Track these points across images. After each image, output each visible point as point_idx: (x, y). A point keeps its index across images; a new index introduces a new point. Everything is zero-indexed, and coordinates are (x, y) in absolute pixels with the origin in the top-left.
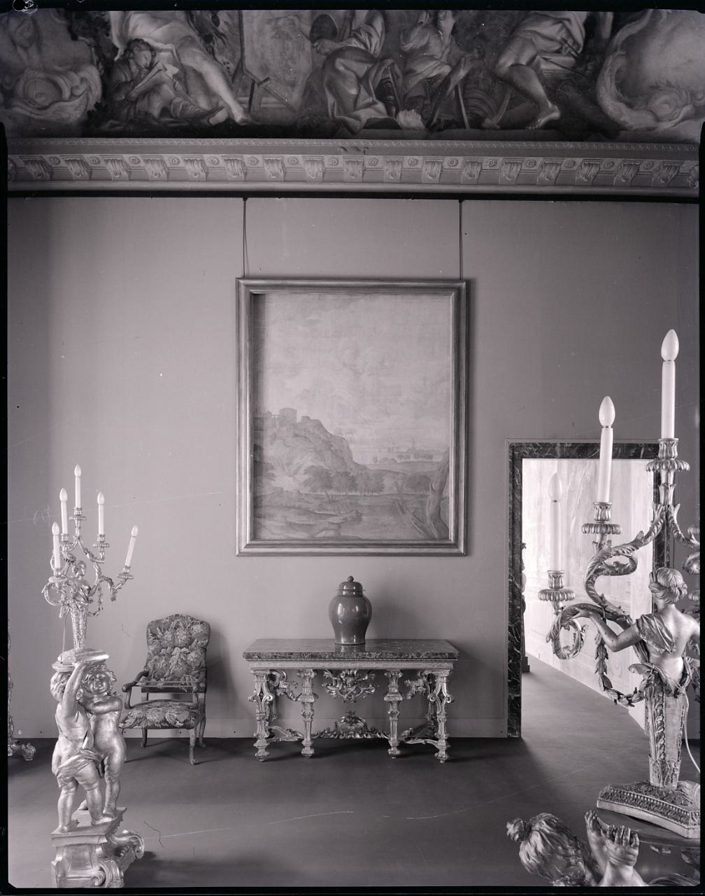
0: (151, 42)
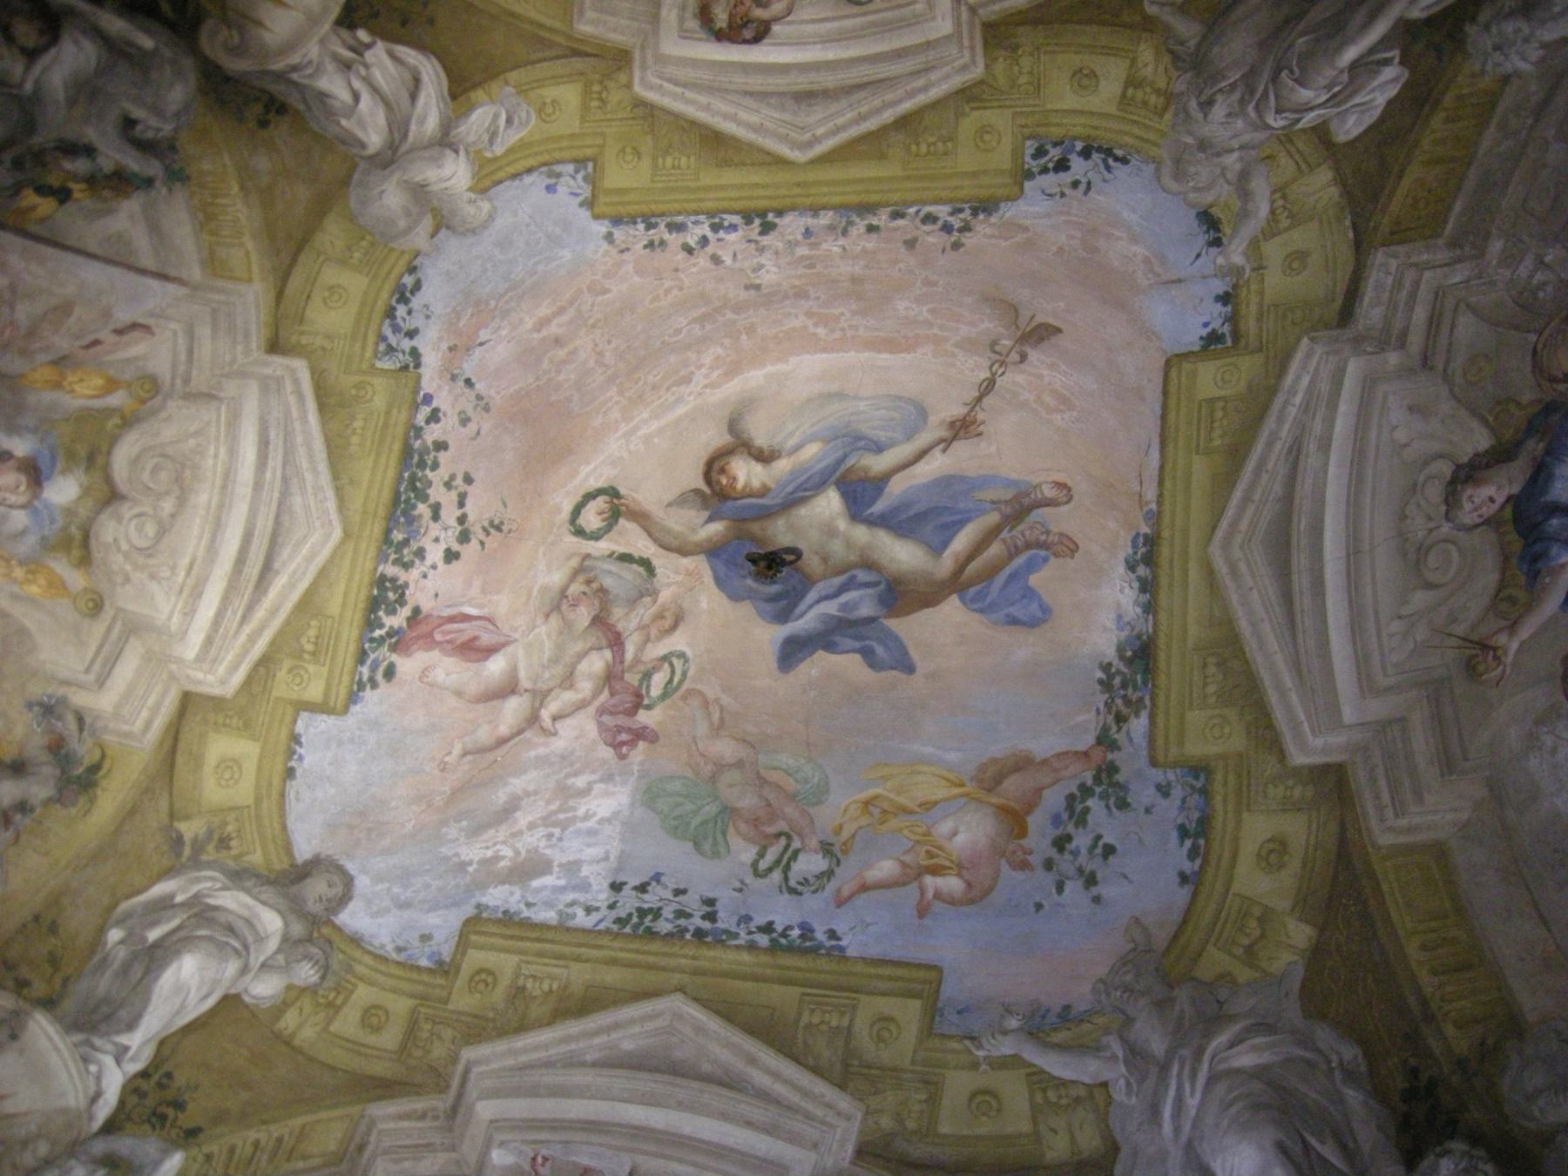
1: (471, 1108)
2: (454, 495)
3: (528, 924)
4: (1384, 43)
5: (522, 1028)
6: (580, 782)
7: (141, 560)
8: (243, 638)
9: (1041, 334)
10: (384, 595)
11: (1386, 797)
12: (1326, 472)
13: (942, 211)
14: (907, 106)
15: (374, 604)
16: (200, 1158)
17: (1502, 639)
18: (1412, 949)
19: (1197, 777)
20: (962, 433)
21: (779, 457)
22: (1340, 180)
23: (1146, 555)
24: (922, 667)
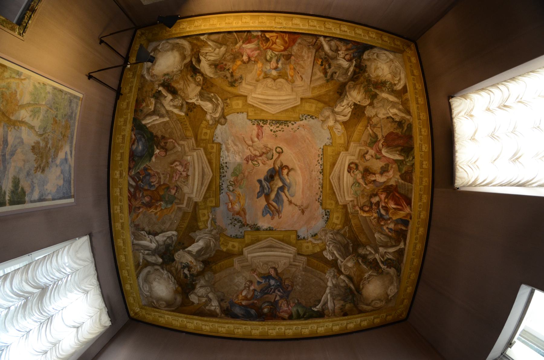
0: (344, 60)
3: (220, 151)
4: (336, 257)
5: (206, 155)
6: (241, 154)
9: (303, 212)
10: (265, 121)
13: (321, 198)
14: (336, 193)
15: (263, 120)
18: (223, 262)
22: (318, 252)
23: (270, 229)
24: (257, 200)
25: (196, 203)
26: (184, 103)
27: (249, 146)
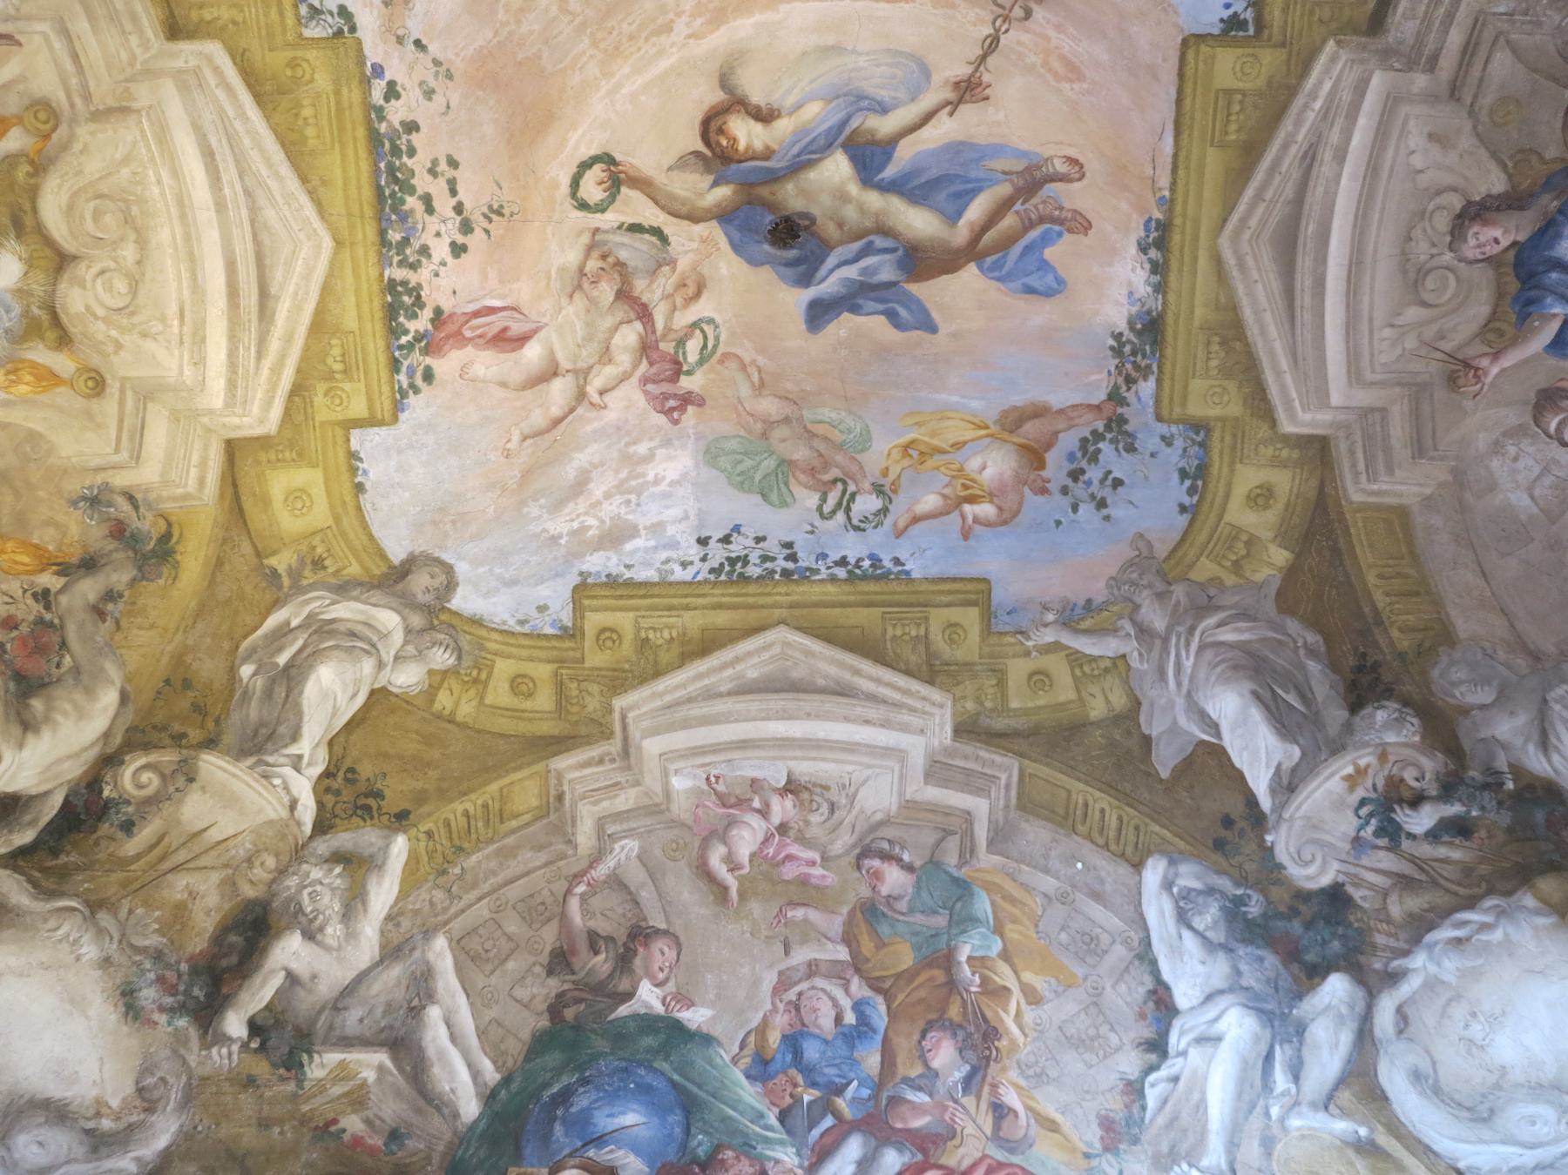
1: (639, 748)
2: (442, 183)
3: (629, 583)
5: (657, 674)
6: (642, 449)
7: (125, 321)
8: (265, 373)
10: (398, 301)
11: (1361, 466)
12: (1338, 183)
15: (391, 312)
16: (422, 837)
17: (1485, 362)
18: (1371, 578)
19: (1197, 433)
20: (967, 97)
21: (779, 116)
23: (1159, 241)
24: (945, 328)
25: (966, 730)
26: (323, 846)
27: (581, 395)
